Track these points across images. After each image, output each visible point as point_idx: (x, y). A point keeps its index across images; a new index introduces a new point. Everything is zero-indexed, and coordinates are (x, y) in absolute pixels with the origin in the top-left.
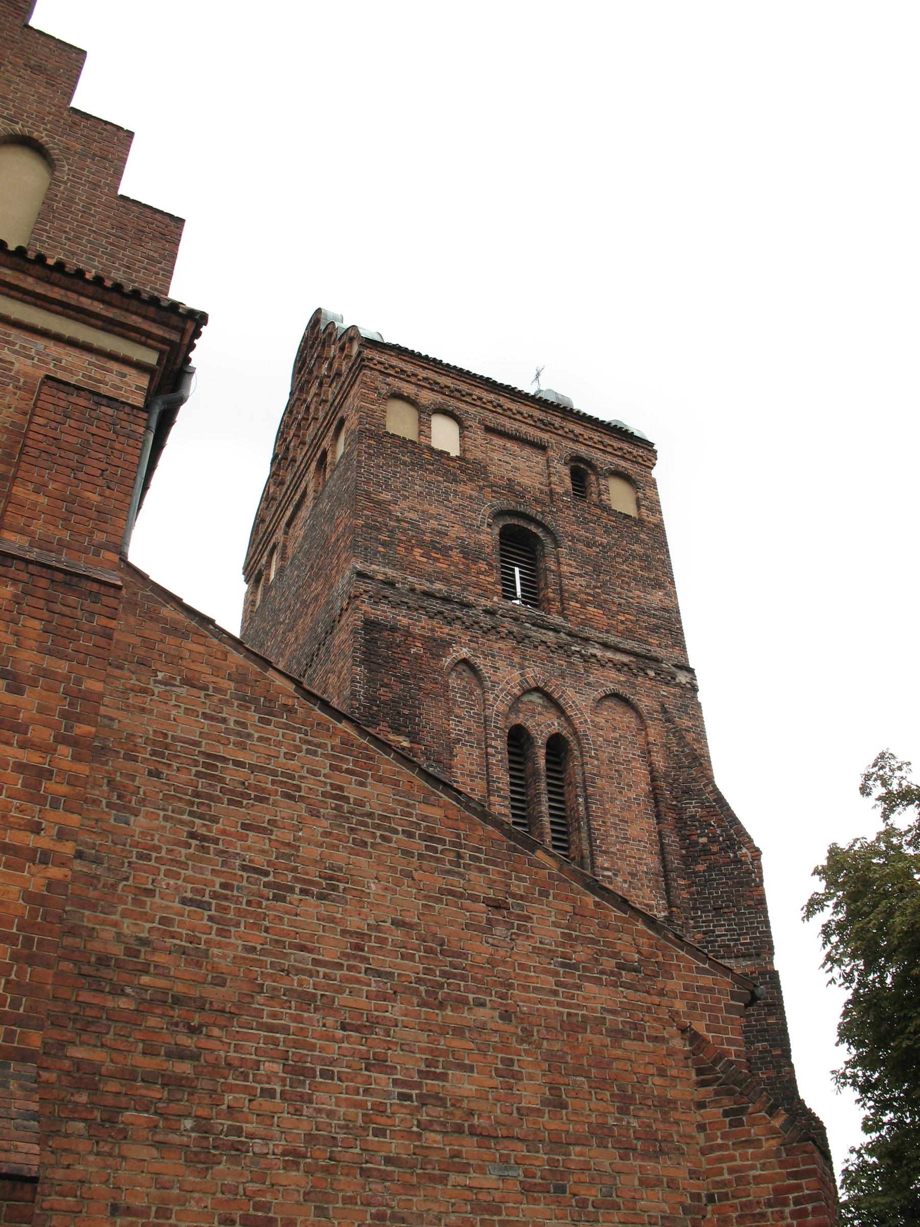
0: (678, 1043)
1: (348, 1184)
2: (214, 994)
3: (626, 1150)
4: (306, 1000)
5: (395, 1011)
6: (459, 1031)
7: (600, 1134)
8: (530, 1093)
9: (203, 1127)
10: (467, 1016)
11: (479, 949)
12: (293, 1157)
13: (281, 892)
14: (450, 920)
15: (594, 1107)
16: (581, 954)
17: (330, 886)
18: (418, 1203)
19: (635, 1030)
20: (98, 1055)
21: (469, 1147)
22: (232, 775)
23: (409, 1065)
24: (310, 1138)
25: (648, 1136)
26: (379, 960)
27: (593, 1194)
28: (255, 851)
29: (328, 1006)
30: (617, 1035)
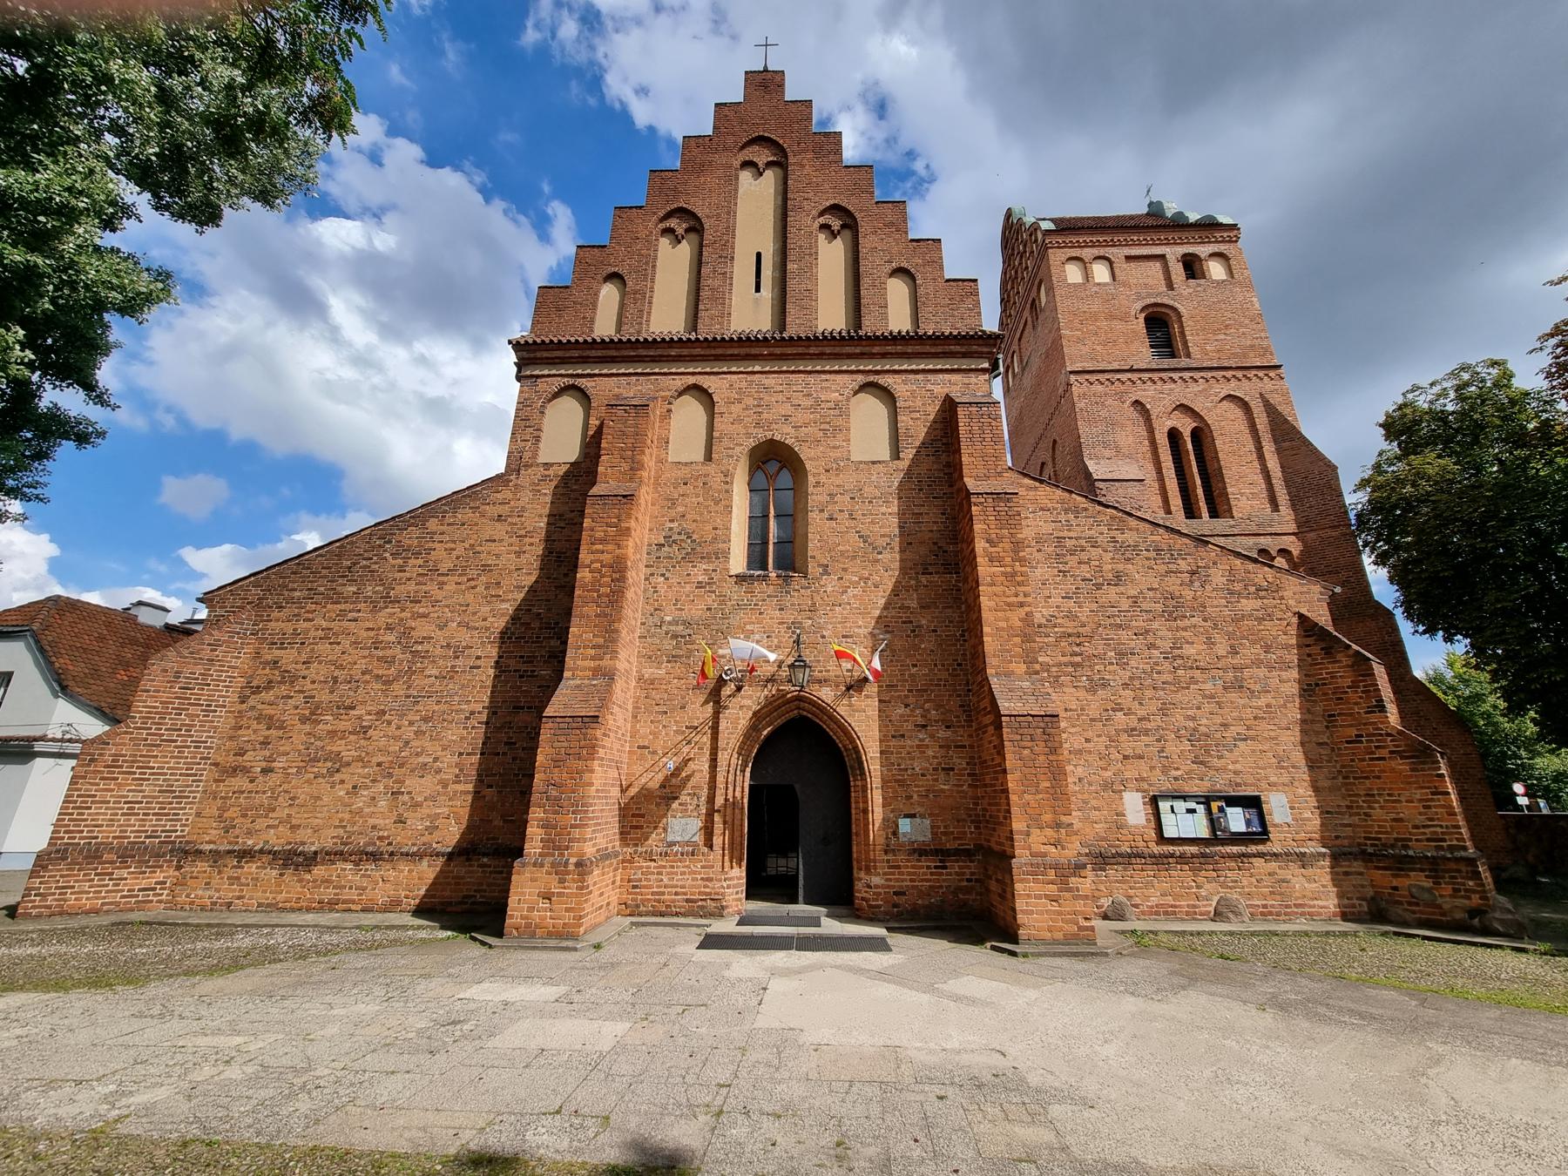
1: (1149, 693)
3: (1271, 668)
5: (1155, 625)
6: (1185, 629)
7: (1258, 663)
8: (1221, 649)
9: (1090, 679)
10: (1187, 622)
13: (1098, 587)
14: (1172, 584)
15: (1250, 652)
16: (1238, 587)
20: (1047, 659)
22: (1069, 543)
24: (1131, 678)
26: (1145, 606)
27: (1258, 687)
28: (1085, 571)
29: (1128, 627)
30: (1260, 620)
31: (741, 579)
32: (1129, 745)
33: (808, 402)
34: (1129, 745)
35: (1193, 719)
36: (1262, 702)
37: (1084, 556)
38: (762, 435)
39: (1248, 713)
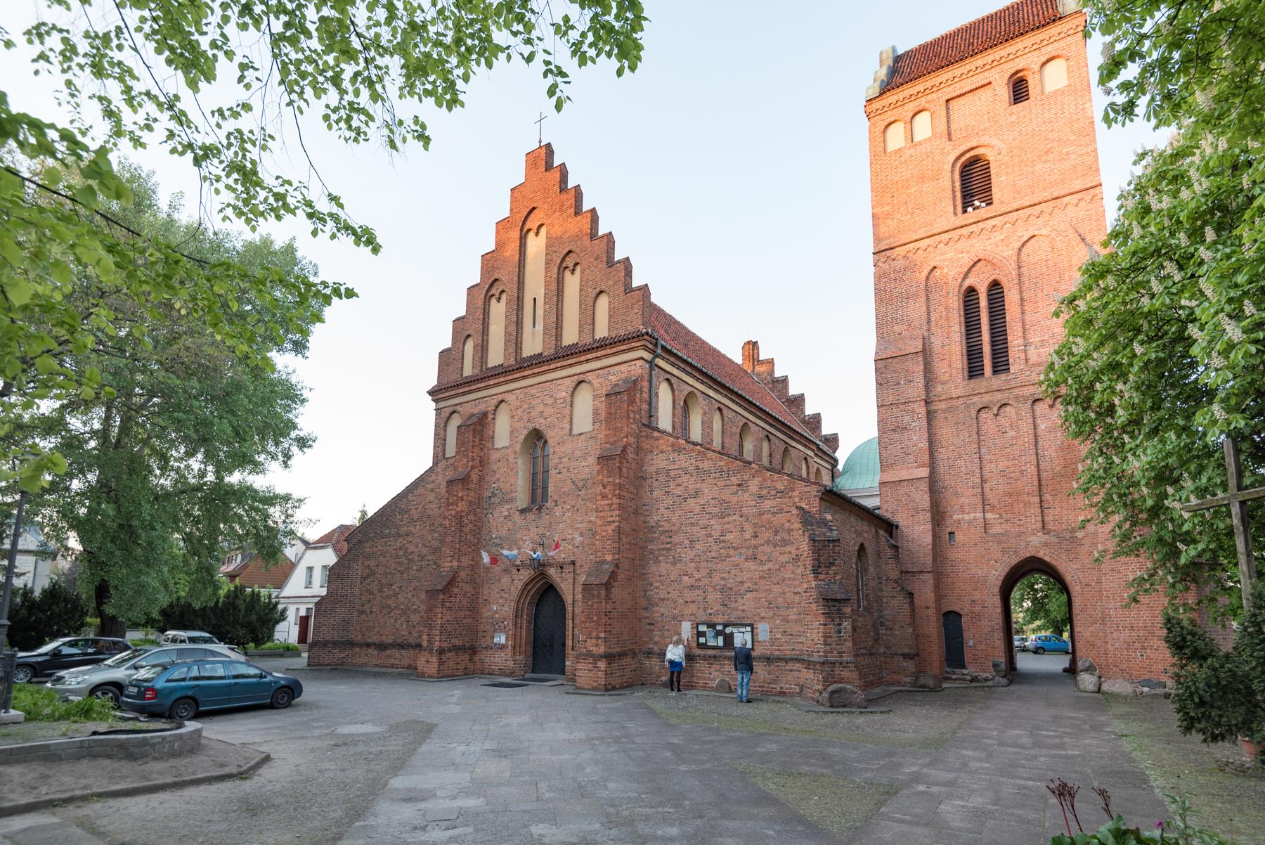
0: (795, 511)
2: (673, 528)
3: (775, 545)
4: (692, 524)
5: (713, 522)
7: (768, 542)
8: (748, 535)
11: (734, 499)
12: (692, 560)
15: (767, 535)
16: (764, 492)
17: (697, 494)
18: (719, 566)
19: (781, 510)
21: (731, 552)
22: (672, 473)
23: (716, 534)
25: (783, 540)
26: (709, 510)
28: (679, 491)
30: (774, 514)
31: (522, 511)
32: (689, 596)
33: (550, 401)
34: (689, 596)
35: (723, 579)
36: (765, 568)
37: (679, 481)
38: (531, 426)
39: (756, 575)
